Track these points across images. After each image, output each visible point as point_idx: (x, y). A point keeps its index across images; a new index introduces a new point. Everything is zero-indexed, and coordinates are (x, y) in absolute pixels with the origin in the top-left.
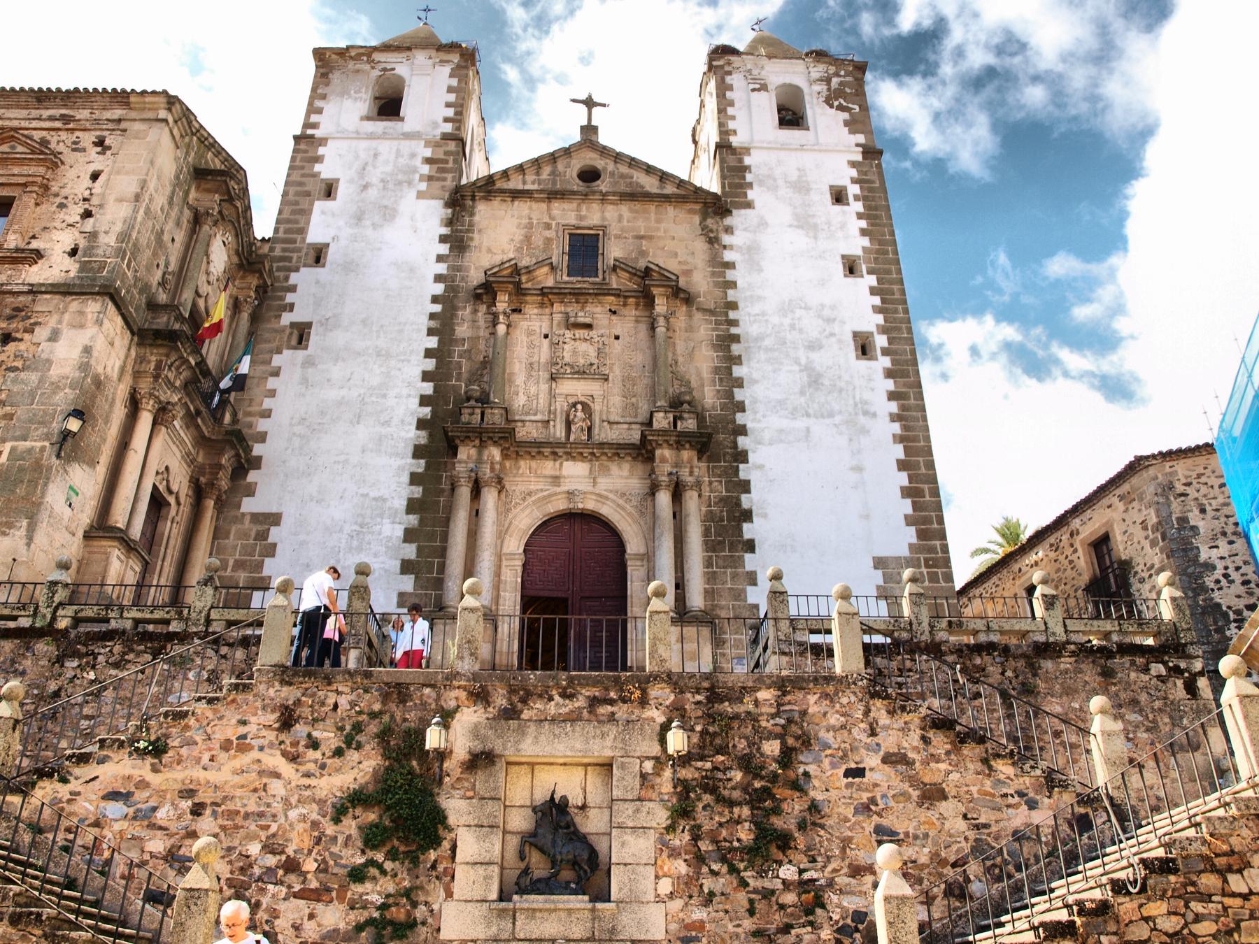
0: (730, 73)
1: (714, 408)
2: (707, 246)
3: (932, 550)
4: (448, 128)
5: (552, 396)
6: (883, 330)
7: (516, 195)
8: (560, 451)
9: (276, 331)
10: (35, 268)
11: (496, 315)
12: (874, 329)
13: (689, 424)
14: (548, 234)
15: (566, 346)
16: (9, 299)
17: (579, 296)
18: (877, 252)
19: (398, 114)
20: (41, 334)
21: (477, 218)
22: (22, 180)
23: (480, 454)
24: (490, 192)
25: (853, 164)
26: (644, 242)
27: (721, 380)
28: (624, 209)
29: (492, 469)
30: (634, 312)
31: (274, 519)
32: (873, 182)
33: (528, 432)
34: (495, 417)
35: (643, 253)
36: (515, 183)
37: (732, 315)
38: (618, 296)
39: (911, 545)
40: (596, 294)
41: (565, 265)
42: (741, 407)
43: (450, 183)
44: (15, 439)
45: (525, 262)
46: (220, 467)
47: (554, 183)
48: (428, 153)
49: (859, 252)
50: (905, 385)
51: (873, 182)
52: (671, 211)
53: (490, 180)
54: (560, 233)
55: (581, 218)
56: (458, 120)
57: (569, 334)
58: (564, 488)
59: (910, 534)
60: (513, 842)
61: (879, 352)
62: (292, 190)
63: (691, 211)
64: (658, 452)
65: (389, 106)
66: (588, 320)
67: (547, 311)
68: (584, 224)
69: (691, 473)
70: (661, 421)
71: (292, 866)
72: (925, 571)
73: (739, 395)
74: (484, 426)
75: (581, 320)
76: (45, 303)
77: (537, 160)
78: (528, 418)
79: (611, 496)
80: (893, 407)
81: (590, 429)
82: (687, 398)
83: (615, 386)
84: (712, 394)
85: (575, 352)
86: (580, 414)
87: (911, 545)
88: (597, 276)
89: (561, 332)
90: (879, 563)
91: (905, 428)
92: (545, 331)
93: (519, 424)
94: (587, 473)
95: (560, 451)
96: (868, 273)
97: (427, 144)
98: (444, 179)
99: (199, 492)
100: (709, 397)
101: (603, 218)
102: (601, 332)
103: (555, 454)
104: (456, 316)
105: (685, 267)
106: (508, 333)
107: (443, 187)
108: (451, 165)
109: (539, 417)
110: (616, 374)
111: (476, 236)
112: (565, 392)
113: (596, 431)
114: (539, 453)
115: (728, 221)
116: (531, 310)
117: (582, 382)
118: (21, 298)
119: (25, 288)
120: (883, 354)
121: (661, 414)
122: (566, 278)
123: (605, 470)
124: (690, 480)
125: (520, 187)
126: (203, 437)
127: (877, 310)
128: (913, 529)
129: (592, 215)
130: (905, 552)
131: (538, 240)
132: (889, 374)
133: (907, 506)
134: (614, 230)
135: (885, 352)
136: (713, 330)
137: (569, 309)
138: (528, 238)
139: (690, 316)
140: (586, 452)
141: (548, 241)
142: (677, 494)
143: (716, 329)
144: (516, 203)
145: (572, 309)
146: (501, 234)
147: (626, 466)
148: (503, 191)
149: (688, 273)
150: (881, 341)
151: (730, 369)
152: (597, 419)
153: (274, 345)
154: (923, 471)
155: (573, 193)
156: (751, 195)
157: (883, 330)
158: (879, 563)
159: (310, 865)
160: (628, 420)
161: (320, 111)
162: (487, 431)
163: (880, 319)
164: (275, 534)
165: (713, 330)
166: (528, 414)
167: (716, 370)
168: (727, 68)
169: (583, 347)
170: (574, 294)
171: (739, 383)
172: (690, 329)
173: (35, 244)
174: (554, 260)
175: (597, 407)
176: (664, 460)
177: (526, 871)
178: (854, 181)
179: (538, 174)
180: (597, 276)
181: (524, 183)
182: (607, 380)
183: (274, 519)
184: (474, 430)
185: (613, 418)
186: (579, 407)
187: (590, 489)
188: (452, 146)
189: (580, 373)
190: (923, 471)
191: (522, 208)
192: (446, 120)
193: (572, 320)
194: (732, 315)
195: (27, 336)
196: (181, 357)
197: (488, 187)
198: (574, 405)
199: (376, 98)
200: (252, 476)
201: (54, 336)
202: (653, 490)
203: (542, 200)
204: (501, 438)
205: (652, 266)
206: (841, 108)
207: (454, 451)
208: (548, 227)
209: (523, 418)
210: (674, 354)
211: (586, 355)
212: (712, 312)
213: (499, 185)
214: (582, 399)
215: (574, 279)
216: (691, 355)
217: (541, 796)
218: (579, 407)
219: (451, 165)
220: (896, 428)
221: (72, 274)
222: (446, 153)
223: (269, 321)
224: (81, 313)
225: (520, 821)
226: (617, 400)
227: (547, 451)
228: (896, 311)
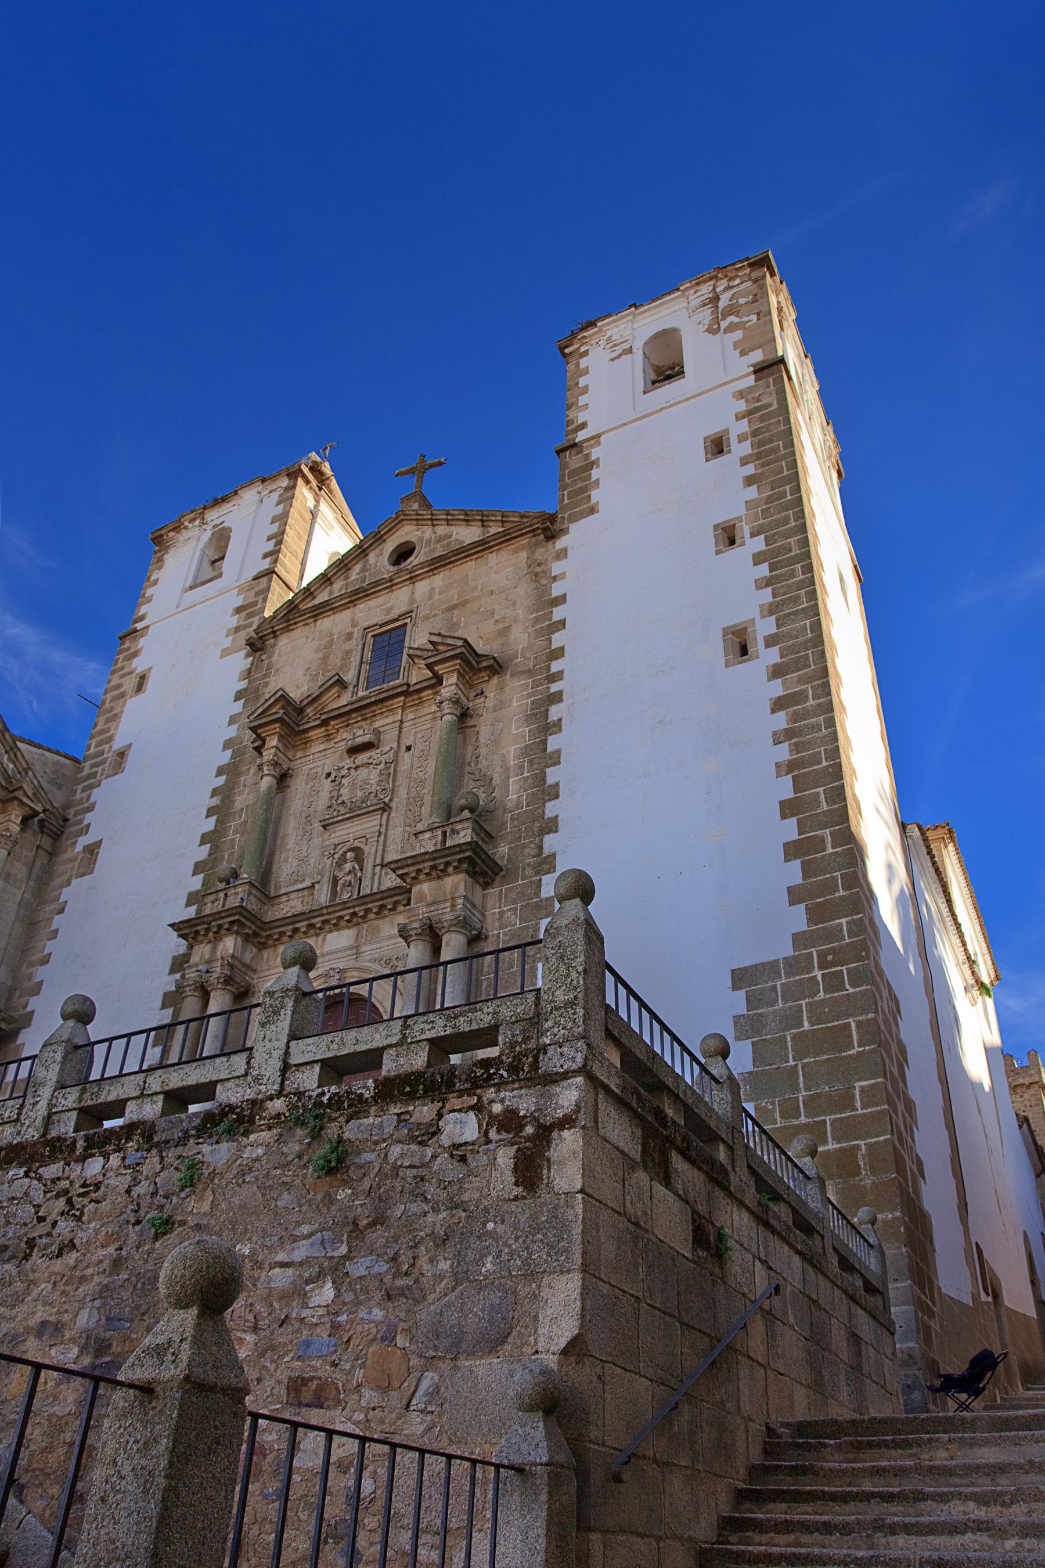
0: (586, 353)
2: (533, 585)
3: (835, 934)
4: (266, 564)
6: (771, 610)
7: (319, 612)
8: (317, 921)
9: (70, 861)
12: (756, 614)
15: (344, 781)
18: (769, 500)
21: (275, 657)
23: (214, 950)
25: (740, 395)
26: (455, 612)
27: (531, 762)
28: (438, 580)
32: (770, 405)
35: (455, 626)
36: (322, 597)
37: (555, 666)
38: (406, 693)
39: (796, 937)
40: (382, 701)
42: (554, 793)
49: (742, 511)
50: (801, 681)
51: (770, 405)
52: (492, 558)
55: (389, 610)
57: (348, 762)
58: (320, 971)
59: (798, 919)
61: (761, 643)
63: (515, 551)
66: (367, 738)
68: (392, 616)
72: (818, 974)
73: (553, 775)
75: (359, 740)
80: (781, 720)
84: (517, 787)
85: (353, 785)
87: (796, 937)
90: (740, 978)
91: (797, 748)
92: (327, 771)
93: (284, 899)
94: (352, 942)
95: (317, 921)
96: (752, 535)
97: (241, 590)
100: (514, 792)
101: (412, 601)
103: (312, 926)
104: (238, 783)
105: (502, 626)
114: (296, 930)
115: (561, 543)
116: (316, 748)
120: (767, 646)
127: (762, 584)
128: (801, 907)
130: (787, 950)
131: (336, 660)
132: (777, 672)
133: (794, 873)
134: (423, 612)
135: (771, 641)
136: (529, 696)
139: (501, 688)
141: (348, 653)
143: (533, 694)
144: (319, 622)
146: (297, 667)
149: (504, 632)
150: (767, 626)
151: (544, 742)
153: (64, 878)
154: (825, 806)
156: (595, 495)
157: (771, 610)
158: (740, 978)
163: (766, 596)
165: (529, 696)
166: (296, 882)
167: (526, 751)
168: (583, 349)
169: (363, 772)
170: (356, 710)
171: (555, 759)
172: (500, 706)
174: (349, 677)
175: (369, 850)
176: (421, 898)
178: (739, 417)
179: (347, 578)
182: (386, 808)
187: (352, 963)
190: (825, 806)
194: (555, 666)
203: (345, 607)
204: (231, 923)
205: (435, 639)
206: (731, 328)
212: (529, 673)
213: (303, 607)
214: (357, 844)
218: (349, 855)
220: (784, 752)
223: (65, 852)
227: (302, 925)
228: (792, 574)
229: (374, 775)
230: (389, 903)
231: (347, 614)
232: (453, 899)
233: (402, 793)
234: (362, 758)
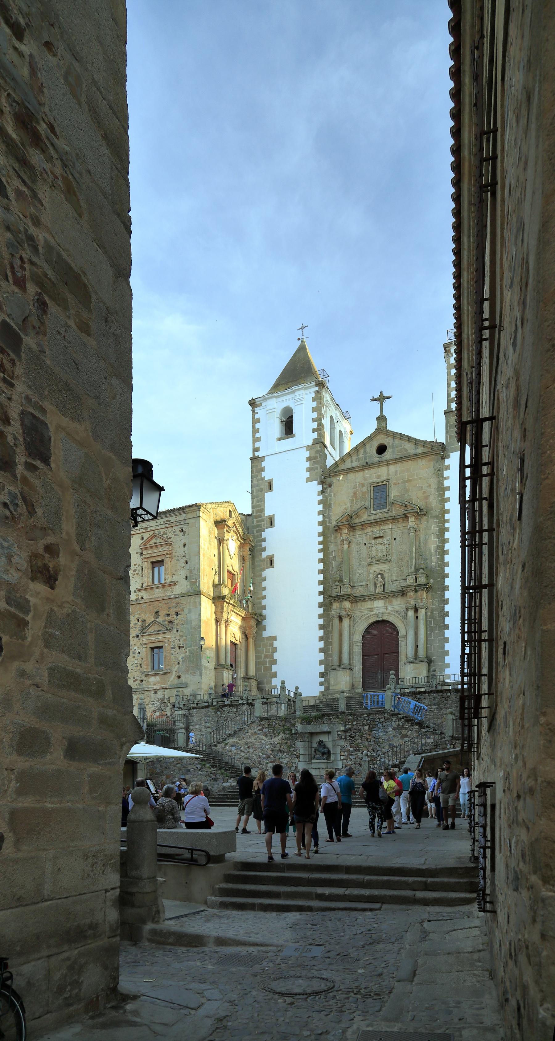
1: (436, 566)
4: (315, 435)
5: (369, 573)
7: (348, 471)
10: (177, 586)
11: (343, 540)
13: (422, 580)
14: (364, 489)
16: (174, 600)
17: (377, 523)
19: (292, 433)
20: (186, 611)
22: (165, 553)
24: (336, 472)
29: (346, 611)
30: (402, 525)
31: (274, 638)
33: (360, 591)
34: (346, 590)
36: (348, 464)
41: (372, 504)
43: (319, 470)
44: (189, 647)
45: (356, 507)
46: (251, 626)
47: (365, 459)
48: (307, 454)
53: (336, 464)
54: (369, 489)
56: (319, 429)
57: (374, 542)
60: (313, 750)
62: (255, 489)
64: (408, 594)
65: (288, 426)
66: (381, 535)
67: (365, 531)
69: (422, 601)
70: (410, 581)
71: (269, 757)
74: (342, 593)
75: (378, 535)
76: (183, 600)
77: (356, 448)
78: (360, 584)
79: (393, 613)
81: (384, 585)
82: (422, 566)
83: (394, 564)
85: (377, 551)
86: (380, 579)
88: (386, 508)
89: (371, 542)
97: (308, 448)
98: (317, 468)
99: (246, 636)
102: (388, 538)
106: (349, 546)
107: (317, 473)
108: (319, 459)
109: (364, 583)
110: (394, 557)
111: (333, 498)
112: (373, 570)
113: (386, 586)
116: (359, 533)
117: (380, 565)
118: (177, 599)
119: (177, 596)
121: (410, 577)
122: (372, 512)
123: (391, 602)
124: (420, 604)
125: (349, 467)
126: (243, 617)
129: (382, 473)
137: (375, 529)
138: (355, 494)
140: (382, 596)
141: (364, 494)
142: (416, 610)
145: (376, 528)
147: (399, 599)
148: (342, 470)
152: (386, 580)
155: (373, 464)
159: (272, 756)
160: (400, 578)
161: (259, 439)
162: (344, 595)
164: (276, 644)
169: (380, 547)
173: (175, 578)
174: (367, 504)
175: (386, 575)
177: (315, 756)
180: (386, 508)
181: (352, 462)
183: (274, 638)
184: (337, 596)
185: (394, 578)
186: (379, 576)
188: (318, 447)
189: (380, 561)
191: (351, 476)
192: (314, 430)
193: (375, 536)
195: (182, 613)
196: (227, 603)
197: (336, 470)
198: (377, 577)
199: (282, 422)
200: (264, 623)
201: (190, 612)
202: (407, 609)
207: (331, 604)
208: (363, 485)
209: (358, 584)
210: (420, 543)
211: (381, 551)
215: (375, 512)
216: (426, 541)
217: (319, 740)
218: (379, 576)
219: (319, 459)
221: (188, 587)
222: (317, 452)
224: (195, 602)
225: (315, 745)
226: (395, 570)
229: (384, 548)
230: (396, 594)
231: (360, 474)
232: (421, 599)
233: (395, 555)
234: (379, 541)
